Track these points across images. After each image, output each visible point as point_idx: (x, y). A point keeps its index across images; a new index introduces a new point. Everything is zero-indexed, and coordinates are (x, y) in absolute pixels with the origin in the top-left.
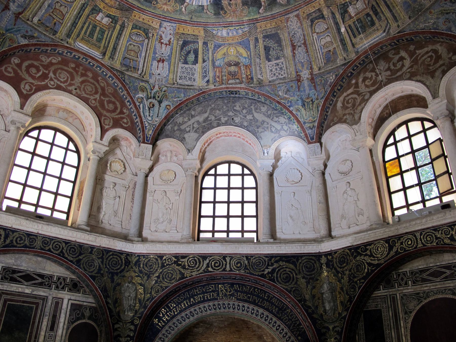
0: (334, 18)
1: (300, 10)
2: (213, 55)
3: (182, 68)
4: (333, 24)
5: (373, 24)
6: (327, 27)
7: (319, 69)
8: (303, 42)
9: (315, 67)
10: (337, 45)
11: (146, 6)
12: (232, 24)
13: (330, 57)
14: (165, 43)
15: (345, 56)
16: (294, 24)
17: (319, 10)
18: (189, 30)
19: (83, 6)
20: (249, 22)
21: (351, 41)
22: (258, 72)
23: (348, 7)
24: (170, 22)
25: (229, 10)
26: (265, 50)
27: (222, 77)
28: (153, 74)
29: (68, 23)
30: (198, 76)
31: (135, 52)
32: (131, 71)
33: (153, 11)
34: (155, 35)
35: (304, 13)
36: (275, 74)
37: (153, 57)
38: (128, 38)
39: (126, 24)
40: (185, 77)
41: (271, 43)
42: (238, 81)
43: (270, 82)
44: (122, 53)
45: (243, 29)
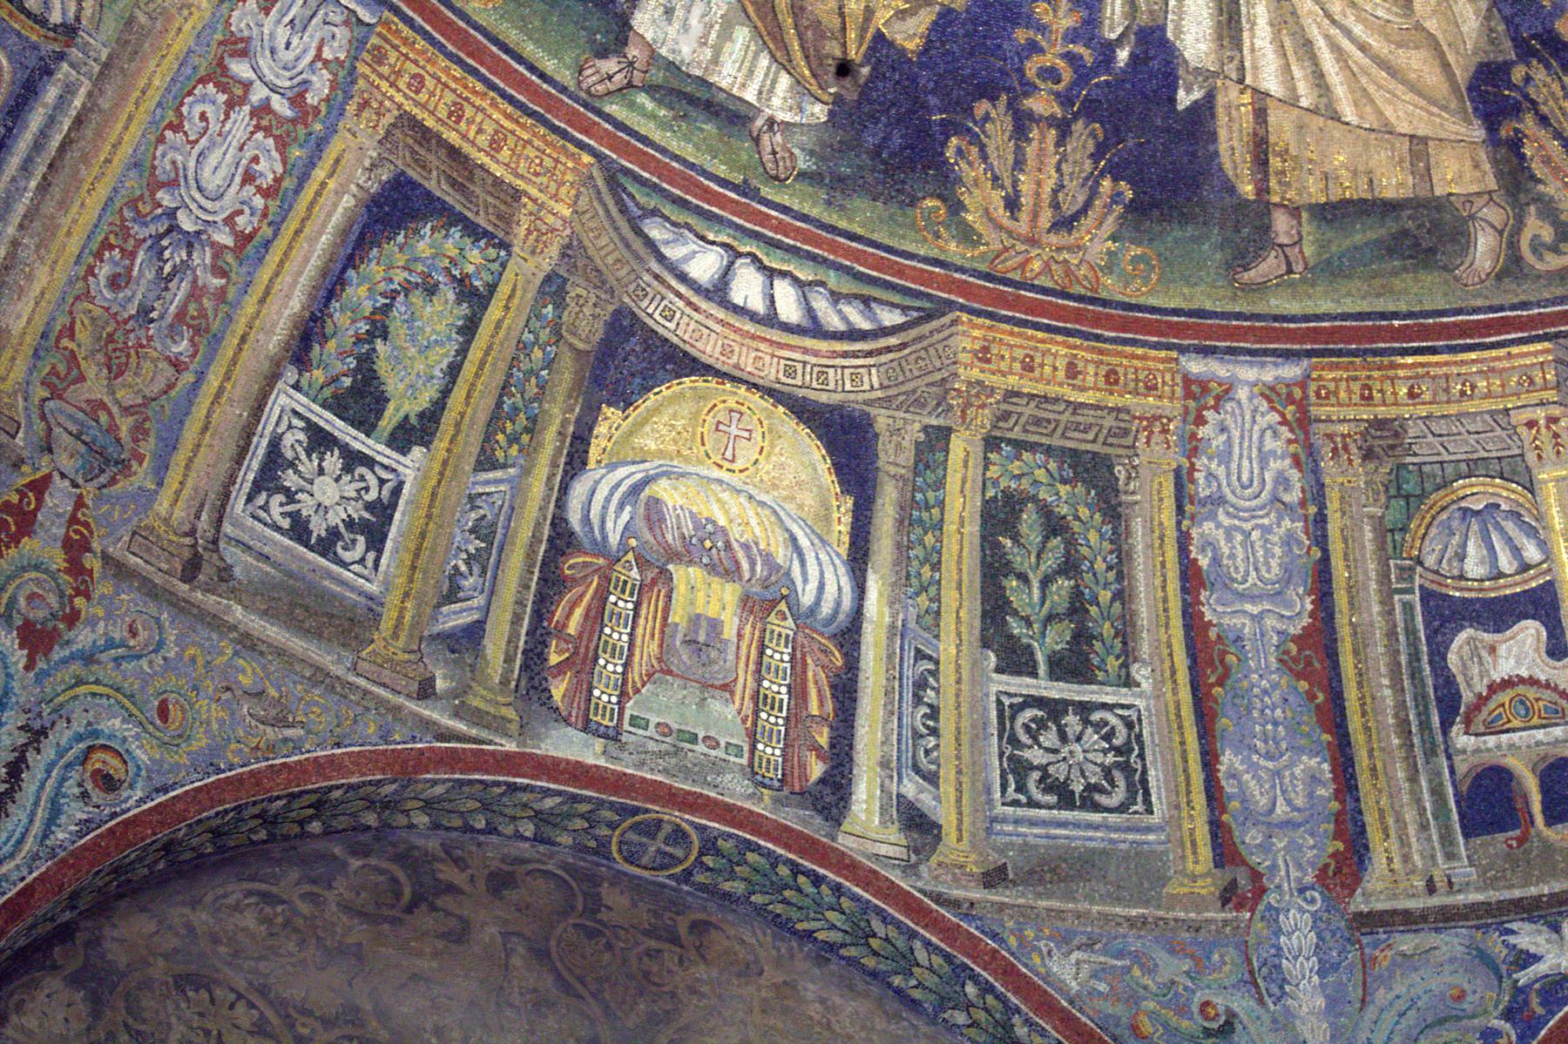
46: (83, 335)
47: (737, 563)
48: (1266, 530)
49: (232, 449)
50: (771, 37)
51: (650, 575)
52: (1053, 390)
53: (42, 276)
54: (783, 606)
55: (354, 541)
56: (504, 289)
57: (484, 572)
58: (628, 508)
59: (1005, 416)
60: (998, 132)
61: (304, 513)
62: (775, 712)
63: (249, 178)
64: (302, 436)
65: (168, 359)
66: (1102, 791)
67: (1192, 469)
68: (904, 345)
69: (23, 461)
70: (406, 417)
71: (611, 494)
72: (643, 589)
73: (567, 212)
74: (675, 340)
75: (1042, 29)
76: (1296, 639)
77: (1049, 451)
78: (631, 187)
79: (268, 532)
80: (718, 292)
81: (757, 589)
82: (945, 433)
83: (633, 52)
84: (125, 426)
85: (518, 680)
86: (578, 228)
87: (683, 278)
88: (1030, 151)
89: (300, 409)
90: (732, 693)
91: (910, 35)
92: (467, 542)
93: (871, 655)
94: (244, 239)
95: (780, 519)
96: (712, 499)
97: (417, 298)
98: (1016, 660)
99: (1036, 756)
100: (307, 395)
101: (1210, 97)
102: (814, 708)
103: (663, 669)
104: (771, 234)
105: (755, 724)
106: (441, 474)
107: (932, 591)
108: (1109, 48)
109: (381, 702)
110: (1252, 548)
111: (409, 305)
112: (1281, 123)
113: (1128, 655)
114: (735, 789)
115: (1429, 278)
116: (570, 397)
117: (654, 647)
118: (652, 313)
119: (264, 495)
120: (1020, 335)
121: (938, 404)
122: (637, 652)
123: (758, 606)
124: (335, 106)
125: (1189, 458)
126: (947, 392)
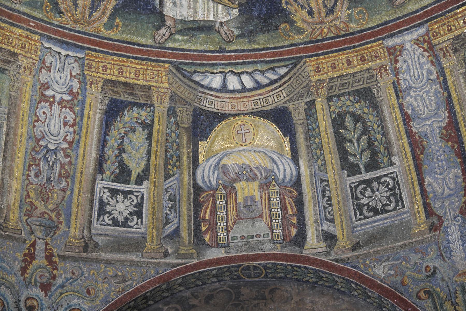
47: (255, 174)
49: (88, 207)
51: (228, 190)
52: (344, 72)
54: (274, 183)
55: (133, 219)
56: (156, 119)
57: (175, 211)
58: (216, 171)
59: (331, 88)
61: (116, 217)
62: (278, 218)
64: (108, 194)
65: (61, 190)
67: (398, 80)
68: (290, 78)
69: (26, 240)
70: (139, 173)
71: (210, 169)
74: (215, 111)
79: (106, 227)
80: (224, 88)
84: (53, 215)
85: (194, 240)
86: (172, 89)
87: (211, 89)
89: (105, 186)
90: (262, 218)
92: (168, 204)
93: (306, 187)
95: (266, 154)
96: (242, 157)
97: (130, 135)
100: (106, 181)
103: (239, 218)
104: (234, 61)
105: (271, 225)
106: (154, 186)
107: (322, 157)
110: (424, 101)
111: (128, 138)
116: (188, 144)
117: (235, 212)
119: (102, 217)
120: (328, 57)
121: (308, 94)
122: (230, 217)
125: (396, 77)
126: (309, 88)
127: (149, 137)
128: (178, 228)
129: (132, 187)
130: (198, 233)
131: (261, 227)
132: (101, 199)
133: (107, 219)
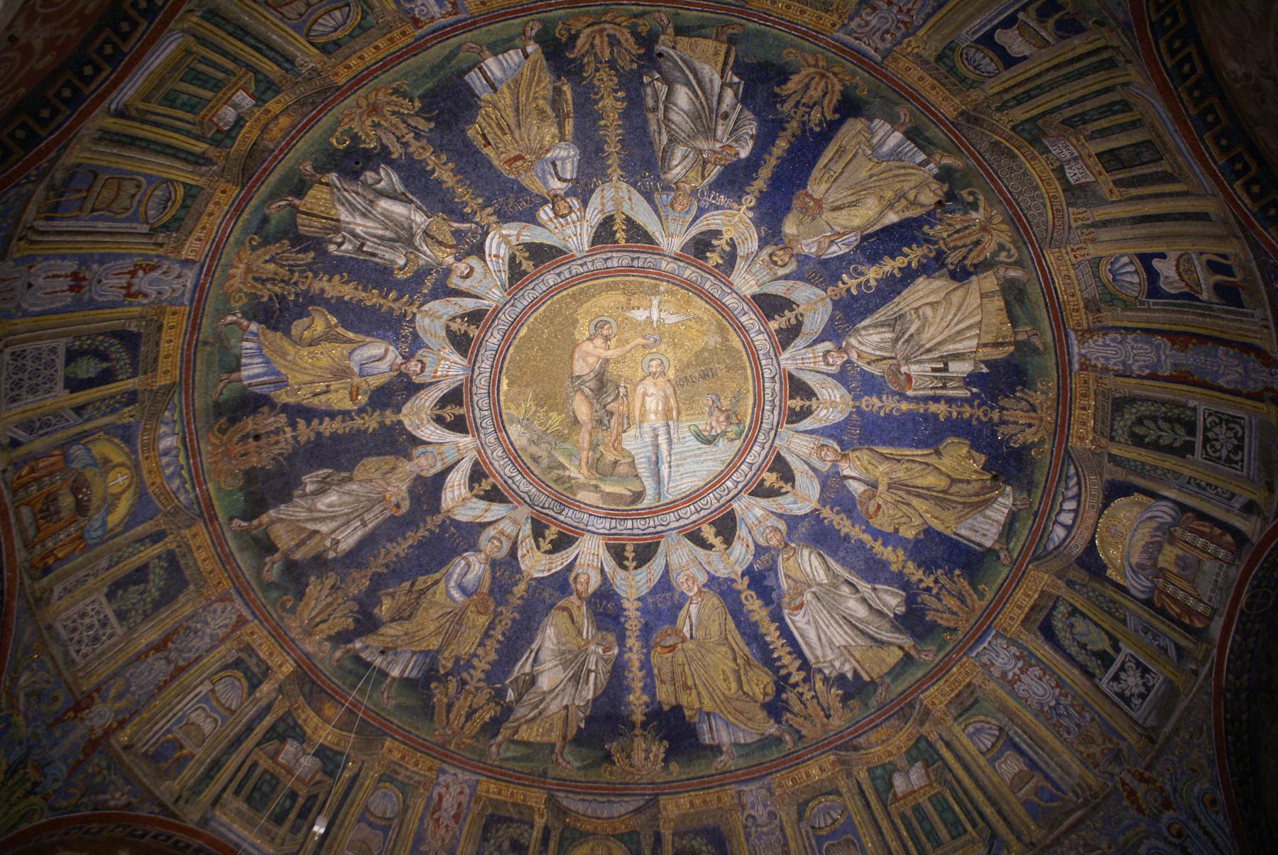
0: (260, 716)
1: (256, 622)
2: (100, 429)
3: (53, 350)
4: (245, 720)
5: (279, 819)
6: (233, 707)
7: (127, 748)
8: (181, 663)
9: (128, 730)
10: (202, 755)
11: (248, 221)
12: (194, 457)
13: (166, 756)
14: (136, 281)
15: (185, 794)
16: (219, 621)
17: (268, 668)
18: (171, 343)
19: (287, 60)
20: (204, 500)
21: (224, 790)
22: (72, 579)
23: (294, 738)
24: (195, 287)
25: (230, 440)
26: (137, 570)
27: (35, 480)
28: (30, 267)
29: (251, 16)
30: (30, 406)
31: (113, 201)
32: (47, 199)
33: (231, 239)
34: (161, 251)
35: (252, 633)
36: (75, 630)
37: (92, 255)
38: (158, 178)
39: (204, 168)
40: (22, 369)
41: (157, 581)
42: (31, 532)
43: (50, 627)
44: (114, 166)
45: (182, 491)
46: (1082, 749)
48: (1133, 348)
50: (987, 503)
53: (1067, 757)
60: (1009, 430)
63: (1040, 679)
66: (1236, 434)
72: (1166, 579)
73: (1046, 576)
75: (971, 416)
76: (1173, 344)
77: (1113, 419)
78: (1038, 553)
80: (1069, 529)
81: (1166, 537)
82: (1110, 455)
83: (997, 547)
84: (1109, 745)
87: (1065, 540)
88: (1011, 419)
91: (983, 458)
94: (1058, 685)
97: (1075, 631)
98: (1189, 448)
99: (1224, 453)
101: (983, 362)
102: (1207, 530)
108: (973, 394)
109: (1198, 691)
110: (1140, 354)
112: (988, 338)
113: (1185, 406)
114: (1235, 573)
115: (1029, 290)
117: (1185, 583)
118: (1077, 551)
123: (1172, 542)
124: (1020, 646)
127: (1084, 616)
128: (1176, 644)
129: (1119, 659)
130: (1189, 629)
131: (1208, 565)
132: (1116, 694)
133: (1136, 701)
